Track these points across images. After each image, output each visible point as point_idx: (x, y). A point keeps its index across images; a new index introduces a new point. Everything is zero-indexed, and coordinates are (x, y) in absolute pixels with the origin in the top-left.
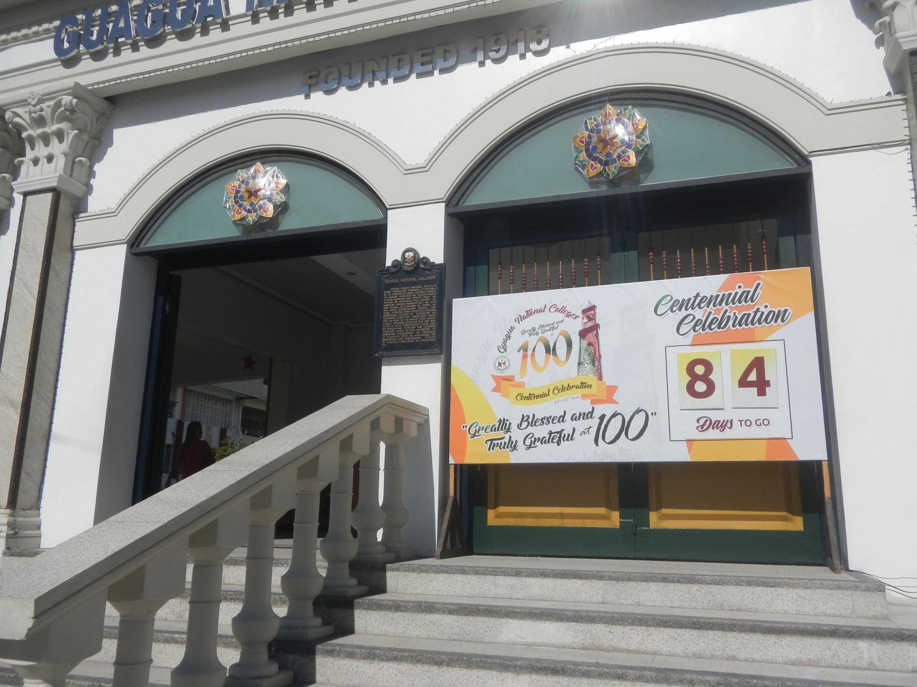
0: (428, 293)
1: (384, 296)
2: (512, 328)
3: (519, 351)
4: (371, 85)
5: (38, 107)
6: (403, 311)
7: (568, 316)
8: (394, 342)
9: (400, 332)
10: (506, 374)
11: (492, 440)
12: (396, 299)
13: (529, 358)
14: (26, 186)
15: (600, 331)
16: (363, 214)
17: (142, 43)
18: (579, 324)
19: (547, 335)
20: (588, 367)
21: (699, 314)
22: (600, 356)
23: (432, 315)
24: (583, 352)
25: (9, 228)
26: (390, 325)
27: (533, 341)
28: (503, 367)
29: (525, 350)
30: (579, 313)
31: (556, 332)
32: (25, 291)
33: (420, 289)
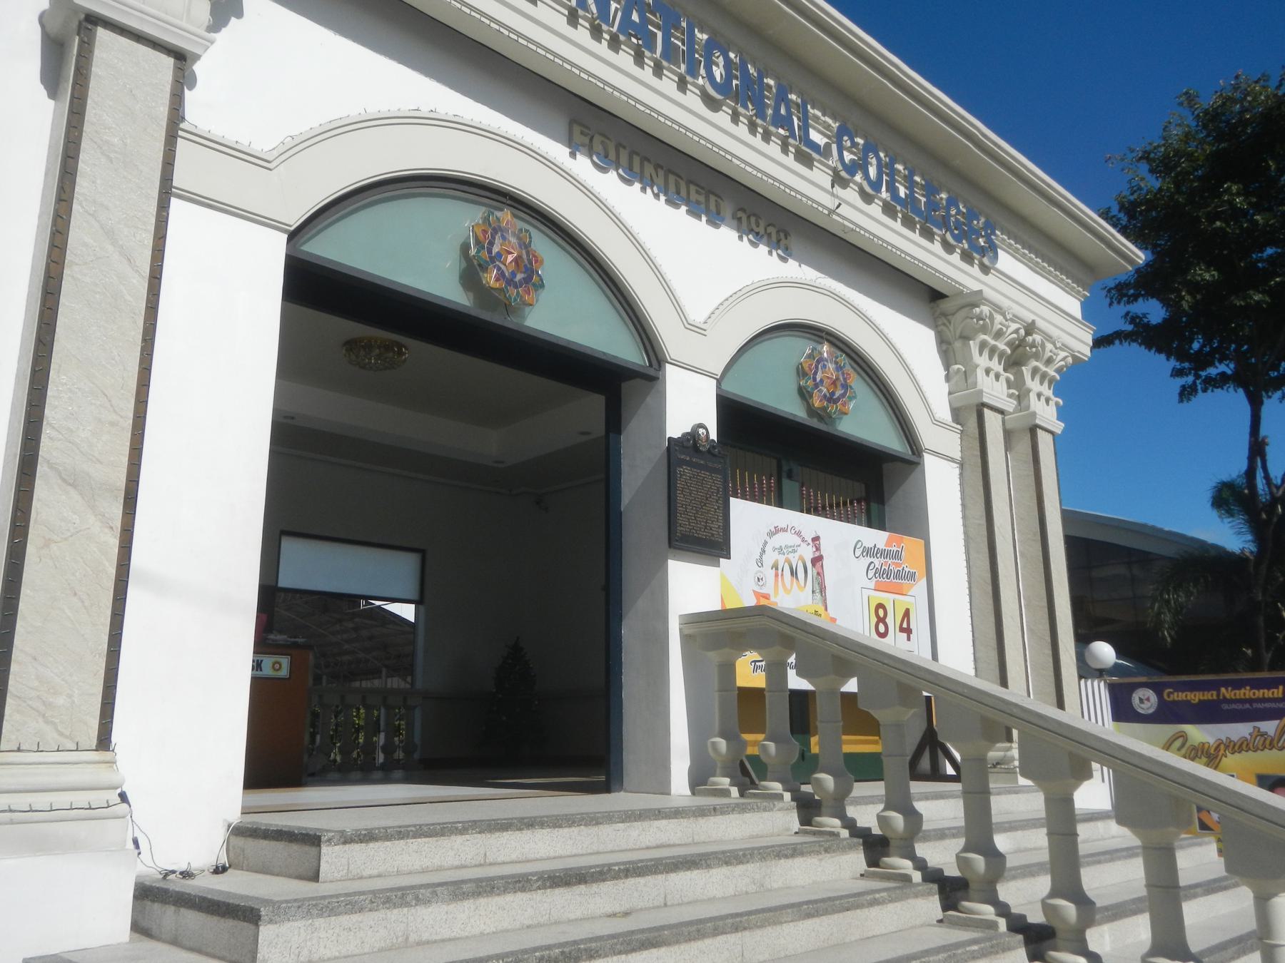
2: (766, 543)
3: (772, 568)
4: (643, 190)
7: (803, 541)
10: (764, 591)
11: (755, 661)
13: (780, 579)
15: (825, 562)
16: (622, 348)
18: (808, 553)
19: (791, 556)
20: (818, 596)
21: (877, 562)
22: (825, 587)
24: (814, 579)
27: (781, 559)
28: (761, 583)
29: (777, 569)
30: (810, 541)
31: (797, 555)
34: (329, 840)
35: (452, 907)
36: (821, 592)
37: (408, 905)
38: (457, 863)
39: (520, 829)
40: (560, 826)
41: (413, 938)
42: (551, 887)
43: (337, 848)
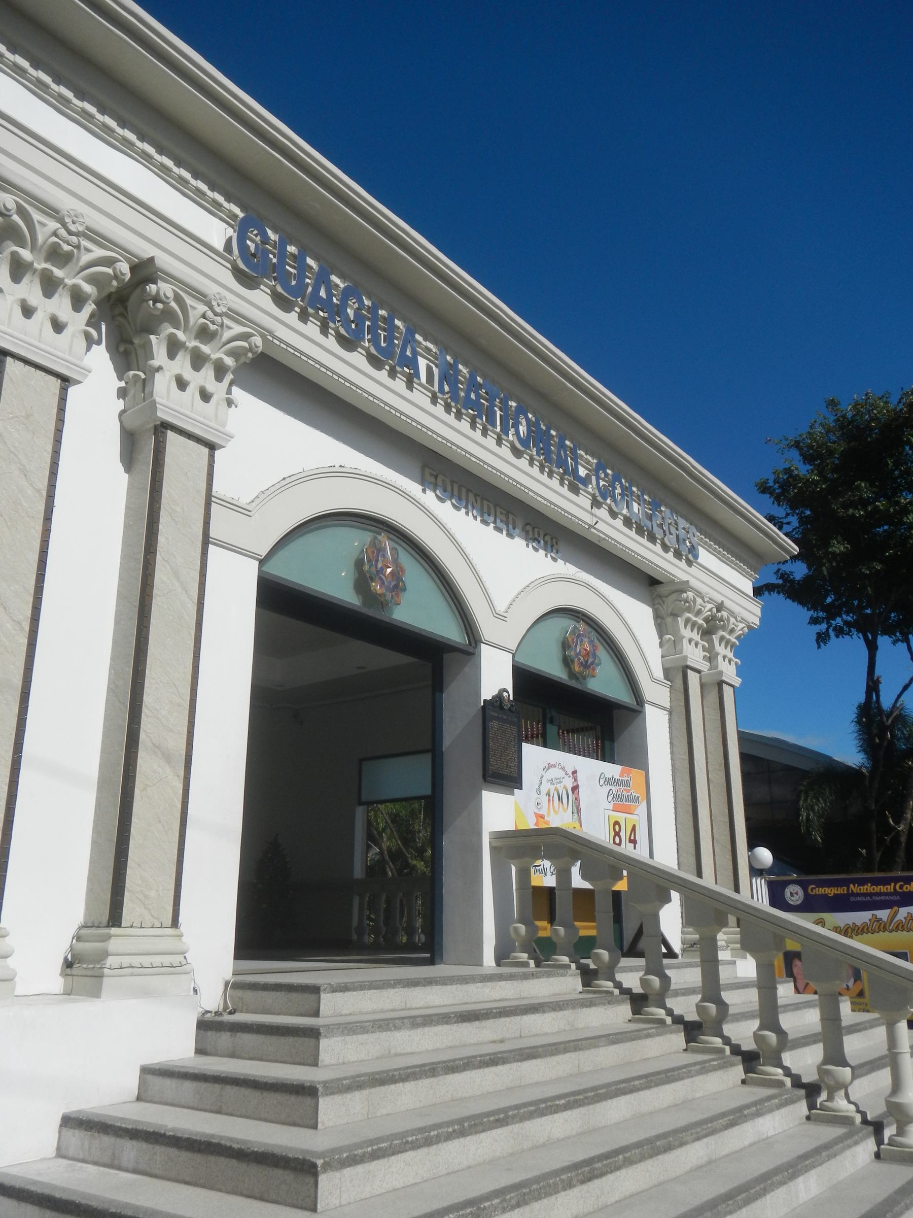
2: (542, 776)
5: (74, 239)
13: (551, 802)
14: (195, 425)
15: (581, 789)
17: (297, 309)
18: (569, 783)
20: (576, 815)
21: (614, 789)
25: (121, 461)
27: (552, 788)
29: (549, 796)
30: (571, 774)
32: (177, 584)
34: (324, 990)
35: (412, 1032)
36: (578, 813)
37: (390, 1030)
38: (391, 1007)
39: (424, 986)
40: (446, 984)
41: (393, 1051)
42: (461, 1022)
43: (329, 995)
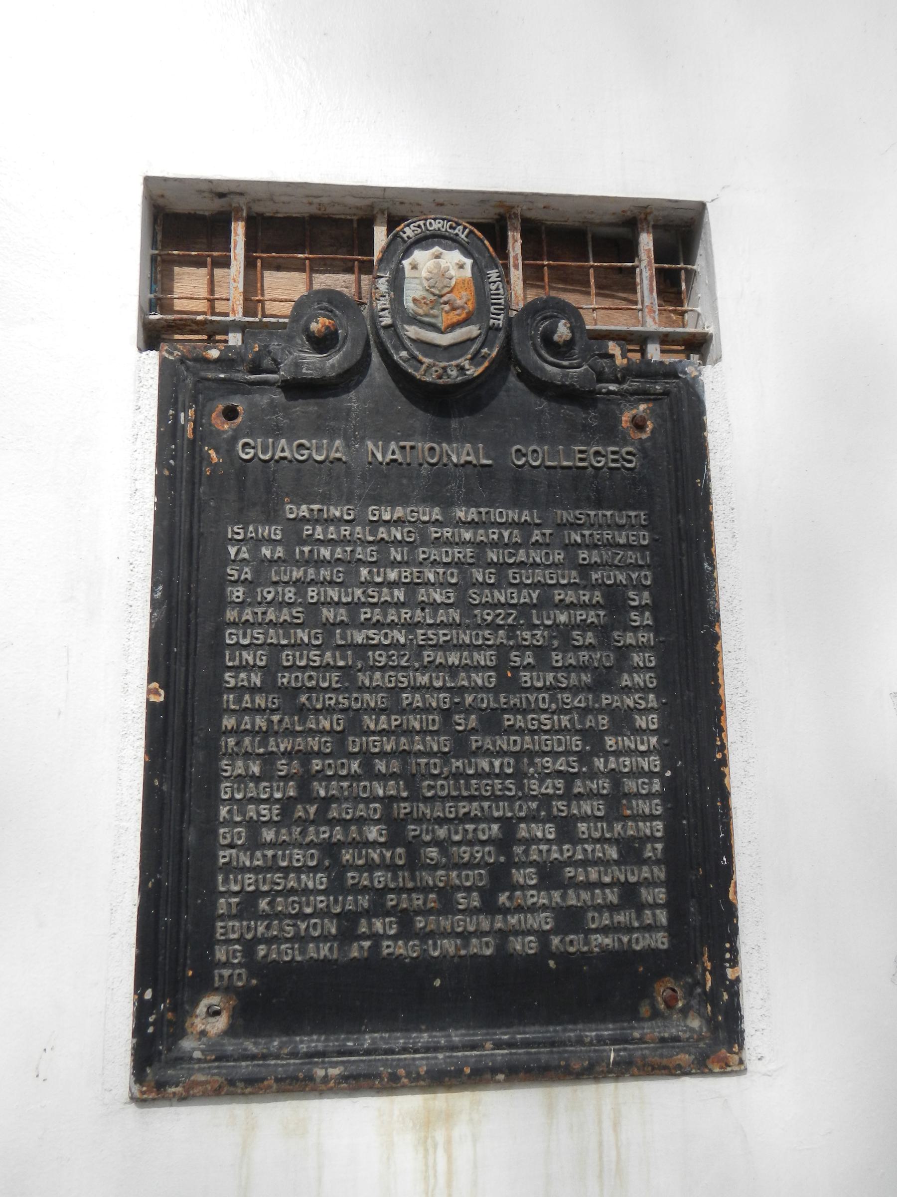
0: (585, 569)
1: (226, 561)
6: (395, 692)
8: (324, 951)
9: (370, 867)
12: (333, 594)
23: (628, 742)
26: (287, 805)
33: (525, 527)
